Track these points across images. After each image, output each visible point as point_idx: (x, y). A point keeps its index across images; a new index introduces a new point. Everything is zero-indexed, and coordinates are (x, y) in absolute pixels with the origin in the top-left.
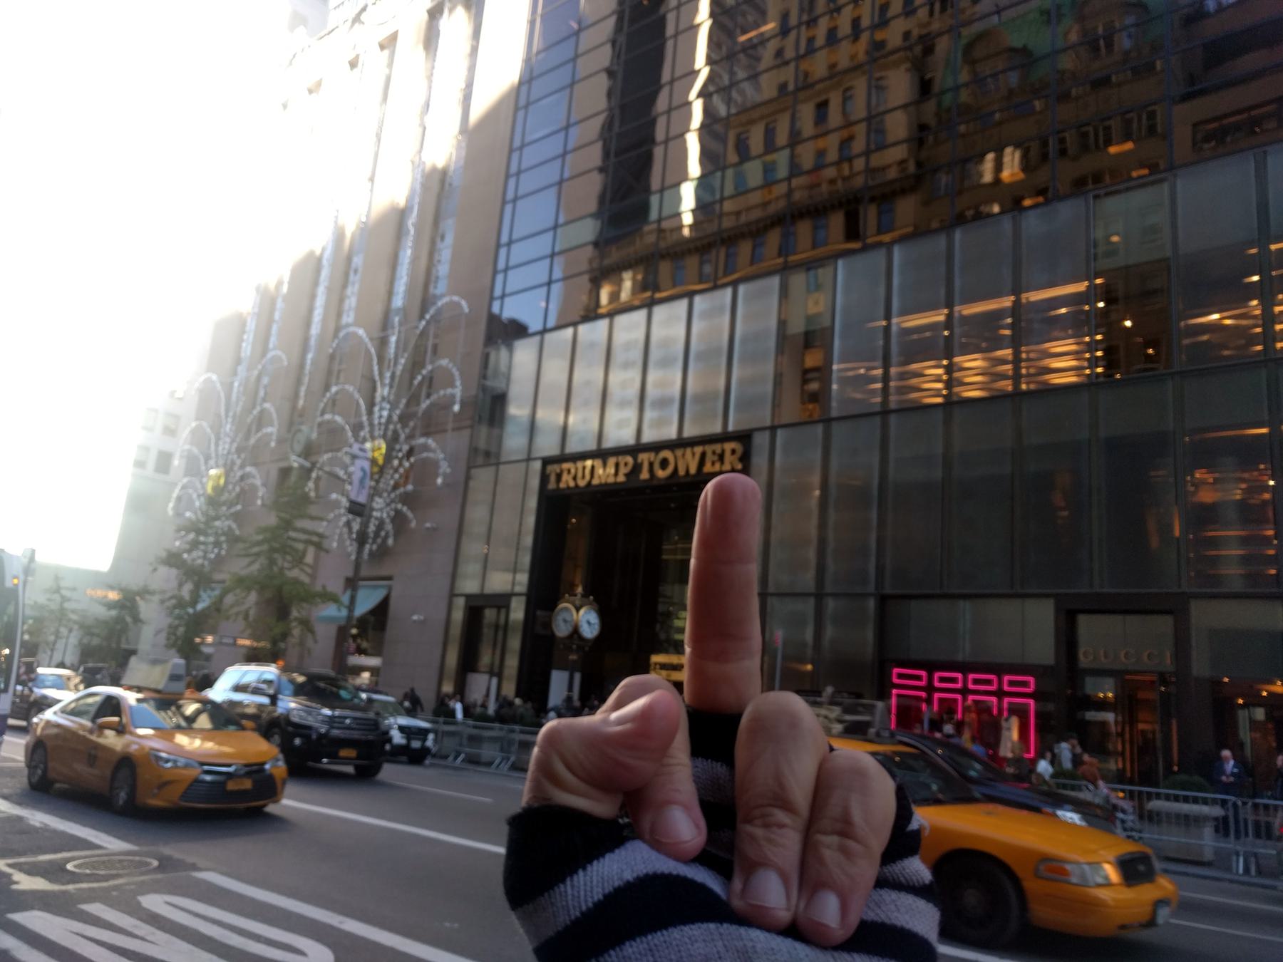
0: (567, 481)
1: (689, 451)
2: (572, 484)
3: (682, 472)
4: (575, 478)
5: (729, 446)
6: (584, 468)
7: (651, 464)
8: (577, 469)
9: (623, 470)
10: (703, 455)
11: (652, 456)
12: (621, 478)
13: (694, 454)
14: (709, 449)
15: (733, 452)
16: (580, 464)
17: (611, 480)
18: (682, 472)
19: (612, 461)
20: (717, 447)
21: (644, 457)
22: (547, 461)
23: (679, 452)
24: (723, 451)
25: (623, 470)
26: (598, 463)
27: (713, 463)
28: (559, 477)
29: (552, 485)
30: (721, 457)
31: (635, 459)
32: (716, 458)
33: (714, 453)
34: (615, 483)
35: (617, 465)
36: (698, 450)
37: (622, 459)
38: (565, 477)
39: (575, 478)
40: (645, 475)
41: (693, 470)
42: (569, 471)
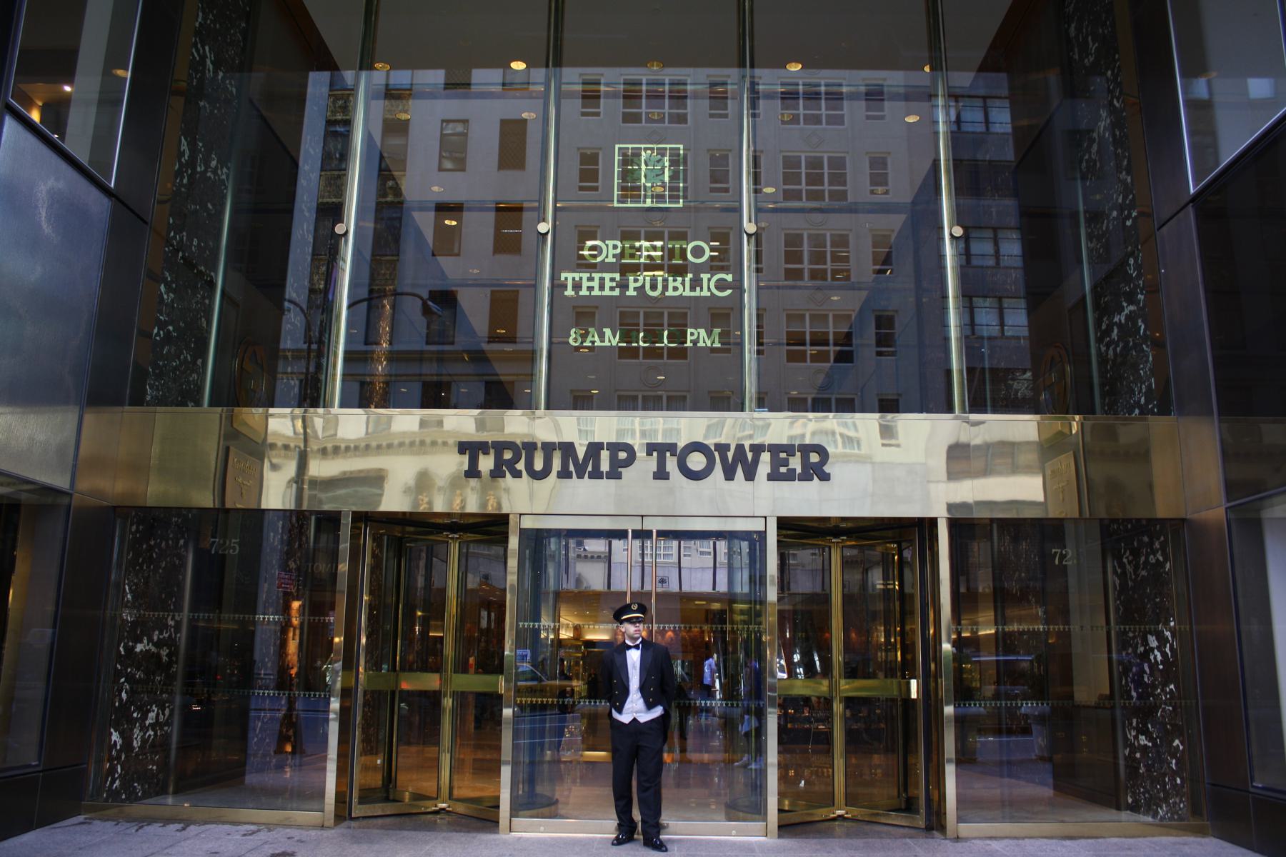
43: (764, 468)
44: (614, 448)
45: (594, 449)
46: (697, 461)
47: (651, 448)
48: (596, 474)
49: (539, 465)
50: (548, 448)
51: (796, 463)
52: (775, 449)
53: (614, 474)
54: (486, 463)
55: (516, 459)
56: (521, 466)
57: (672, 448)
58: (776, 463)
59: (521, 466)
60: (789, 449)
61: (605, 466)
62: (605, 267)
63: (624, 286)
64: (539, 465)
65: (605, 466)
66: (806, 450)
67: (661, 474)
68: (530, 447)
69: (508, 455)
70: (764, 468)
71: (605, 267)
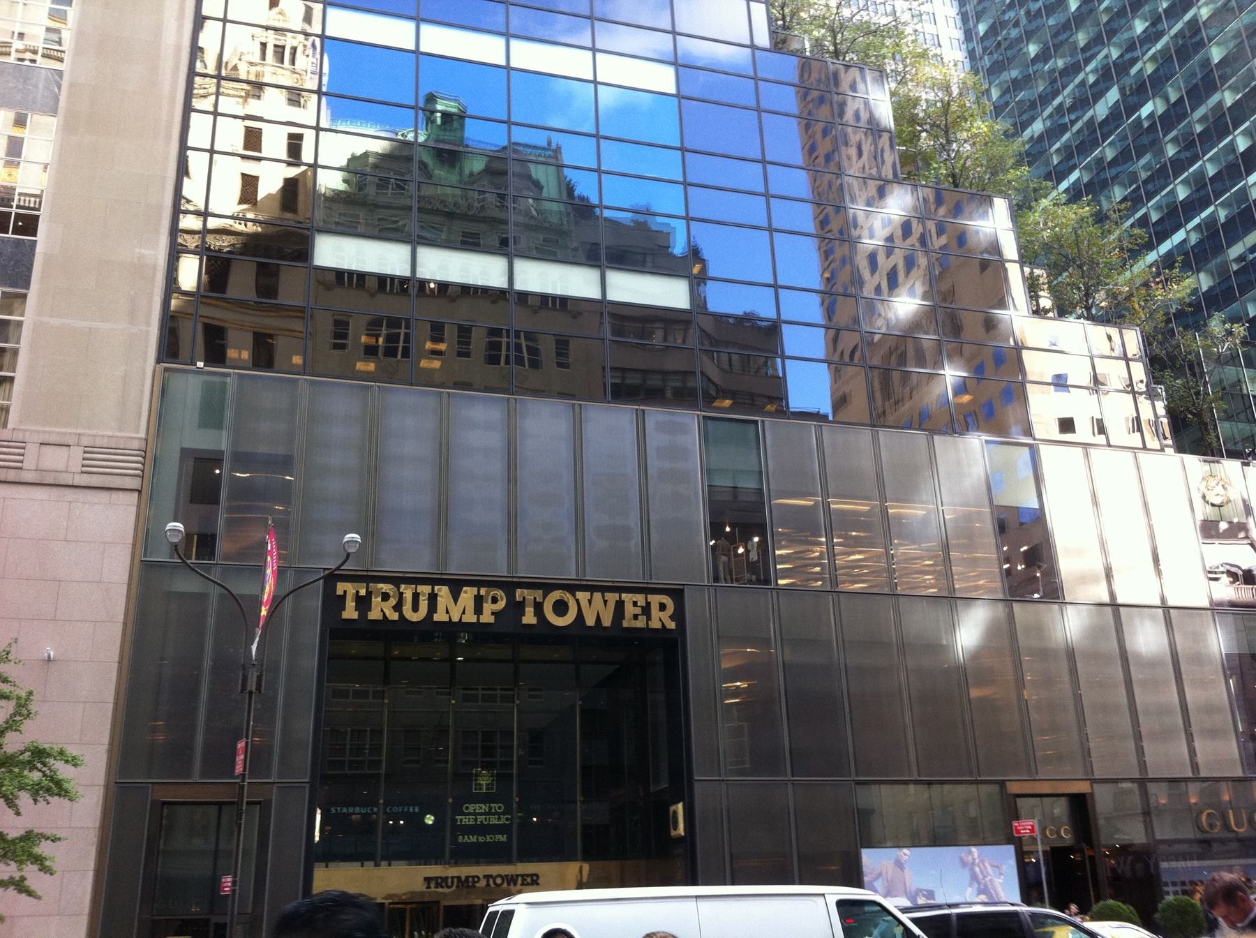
0: (380, 610)
1: (597, 595)
2: (394, 616)
3: (590, 621)
4: (398, 607)
5: (655, 599)
7: (538, 607)
10: (620, 605)
11: (538, 594)
12: (487, 618)
13: (605, 602)
15: (662, 607)
17: (470, 617)
18: (590, 621)
19: (468, 594)
20: (640, 599)
22: (332, 578)
23: (583, 596)
24: (648, 604)
25: (488, 607)
26: (443, 592)
28: (363, 603)
29: (350, 612)
30: (646, 610)
32: (638, 610)
33: (635, 604)
34: (478, 623)
35: (479, 601)
36: (612, 597)
38: (376, 600)
39: (398, 607)
40: (529, 618)
41: (607, 621)
43: (520, 881)
44: (473, 877)
45: (467, 877)
46: (499, 881)
47: (485, 876)
51: (529, 880)
52: (522, 876)
57: (491, 876)
58: (523, 880)
60: (527, 875)
62: (470, 814)
63: (476, 820)
66: (532, 875)
70: (520, 881)
71: (470, 814)
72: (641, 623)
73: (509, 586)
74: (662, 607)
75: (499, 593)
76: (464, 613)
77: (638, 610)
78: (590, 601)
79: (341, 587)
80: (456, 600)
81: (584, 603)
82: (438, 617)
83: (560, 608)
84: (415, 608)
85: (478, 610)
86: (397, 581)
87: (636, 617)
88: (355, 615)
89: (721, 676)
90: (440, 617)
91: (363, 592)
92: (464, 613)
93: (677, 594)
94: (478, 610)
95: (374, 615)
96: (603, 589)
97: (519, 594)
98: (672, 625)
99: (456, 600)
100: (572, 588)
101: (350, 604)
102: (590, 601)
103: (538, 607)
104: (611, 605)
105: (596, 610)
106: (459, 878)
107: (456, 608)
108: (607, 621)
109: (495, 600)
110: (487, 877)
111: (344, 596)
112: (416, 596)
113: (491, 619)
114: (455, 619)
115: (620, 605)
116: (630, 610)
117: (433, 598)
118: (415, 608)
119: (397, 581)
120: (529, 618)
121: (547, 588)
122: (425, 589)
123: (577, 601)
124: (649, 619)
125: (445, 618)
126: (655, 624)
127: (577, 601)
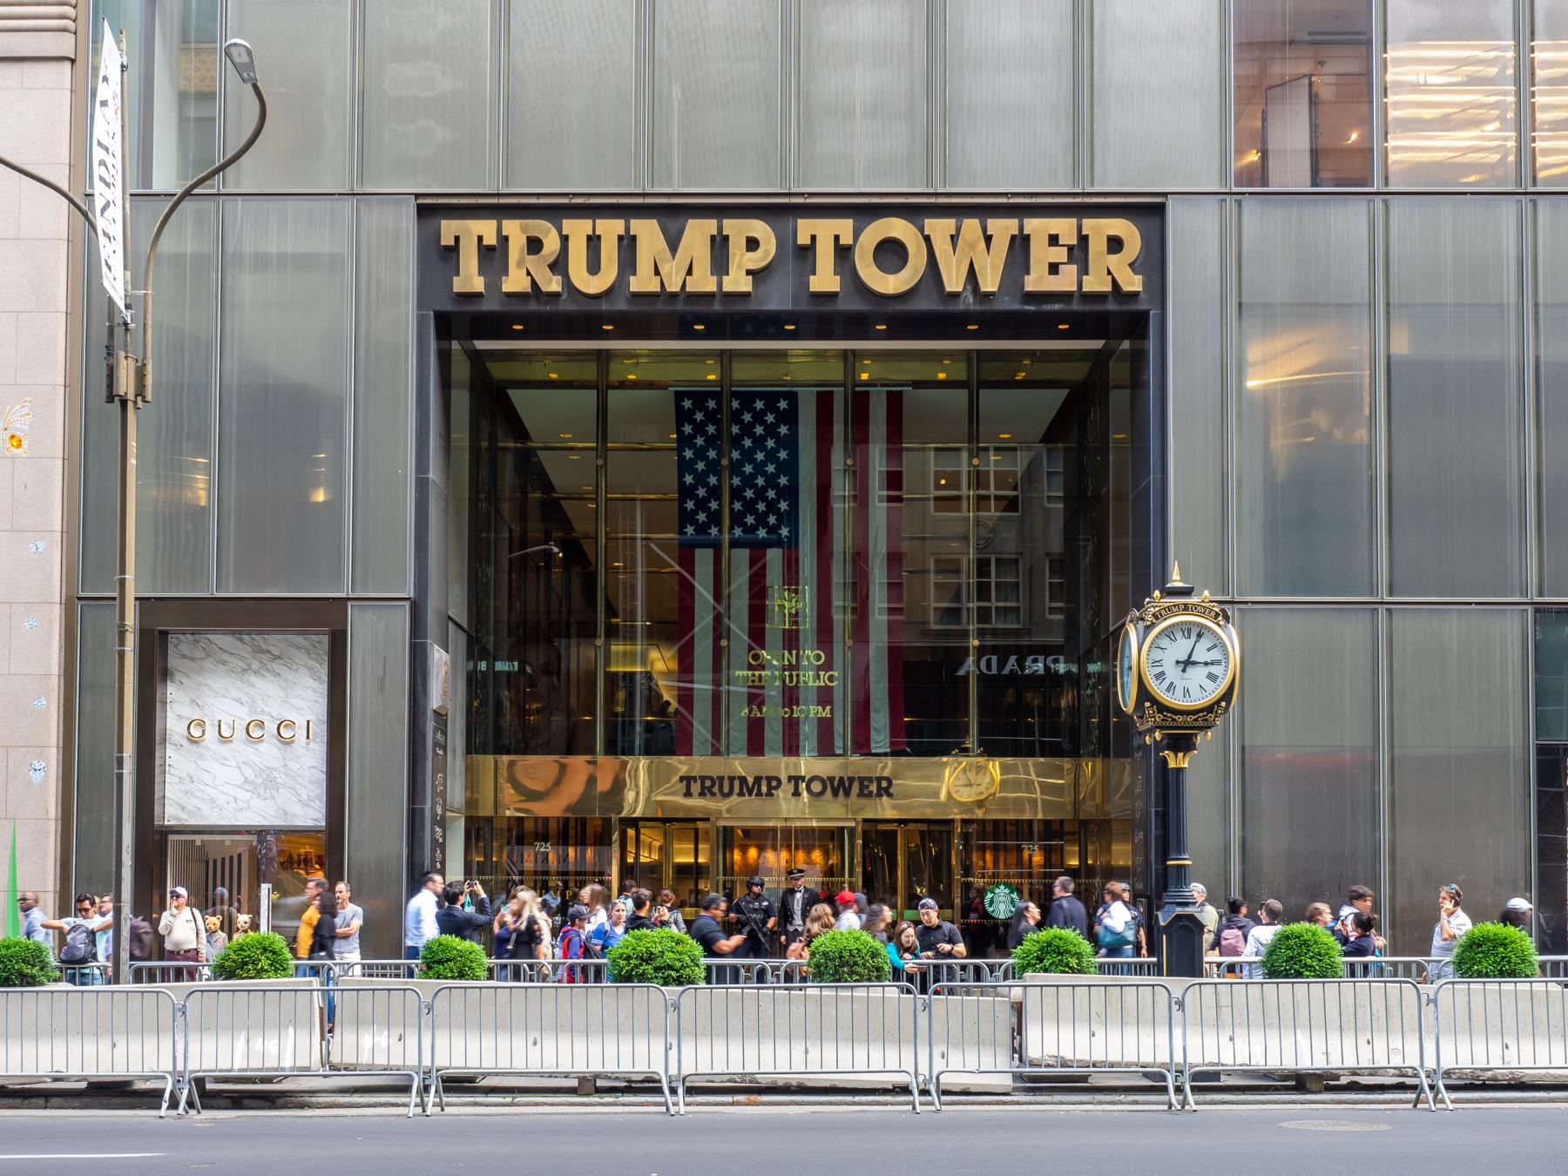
1: (971, 225)
2: (553, 284)
4: (559, 265)
5: (1099, 228)
6: (593, 241)
7: (843, 253)
8: (565, 239)
9: (742, 262)
10: (1021, 243)
11: (844, 227)
13: (988, 239)
14: (1037, 227)
16: (577, 229)
17: (704, 282)
18: (954, 281)
19: (698, 232)
20: (1065, 227)
21: (824, 232)
22: (430, 211)
23: (940, 228)
24: (1083, 240)
25: (742, 262)
26: (648, 232)
27: (1054, 268)
28: (494, 257)
30: (1079, 252)
31: (785, 241)
32: (1060, 254)
33: (1054, 240)
35: (720, 245)
36: (1002, 228)
37: (738, 229)
41: (990, 282)
42: (534, 245)
44: (769, 779)
45: (758, 780)
46: (816, 787)
47: (790, 778)
48: (759, 794)
49: (726, 790)
50: (732, 779)
53: (769, 794)
54: (696, 788)
55: (713, 785)
56: (716, 789)
57: (803, 778)
59: (716, 789)
61: (764, 789)
64: (726, 790)
65: (764, 789)
67: (797, 793)
68: (721, 779)
69: (708, 783)
72: (1066, 281)
73: (779, 212)
74: (1115, 244)
75: (760, 228)
76: (690, 272)
77: (1060, 254)
78: (954, 239)
79: (449, 229)
80: (673, 244)
81: (941, 246)
82: (637, 284)
83: (890, 254)
84: (594, 267)
85: (720, 264)
86: (555, 211)
87: (1054, 268)
88: (478, 284)
89: (1240, 382)
90: (643, 282)
91: (490, 239)
92: (690, 272)
93: (1149, 212)
94: (720, 264)
95: (515, 282)
96: (985, 211)
97: (806, 228)
98: (1133, 283)
99: (673, 244)
100: (914, 211)
101: (469, 259)
102: (954, 239)
103: (843, 253)
104: (1001, 246)
105: (969, 260)
106: (743, 780)
107: (673, 265)
108: (989, 283)
109: (752, 244)
110: (795, 780)
111: (453, 250)
112: (593, 241)
113: (745, 285)
114: (674, 286)
115: (1021, 243)
116: (1041, 254)
117: (628, 244)
118: (594, 267)
119: (555, 211)
120: (825, 279)
121: (865, 211)
122: (611, 228)
123: (927, 239)
124: (1084, 270)
125: (653, 286)
126: (1096, 283)
127: (927, 239)
